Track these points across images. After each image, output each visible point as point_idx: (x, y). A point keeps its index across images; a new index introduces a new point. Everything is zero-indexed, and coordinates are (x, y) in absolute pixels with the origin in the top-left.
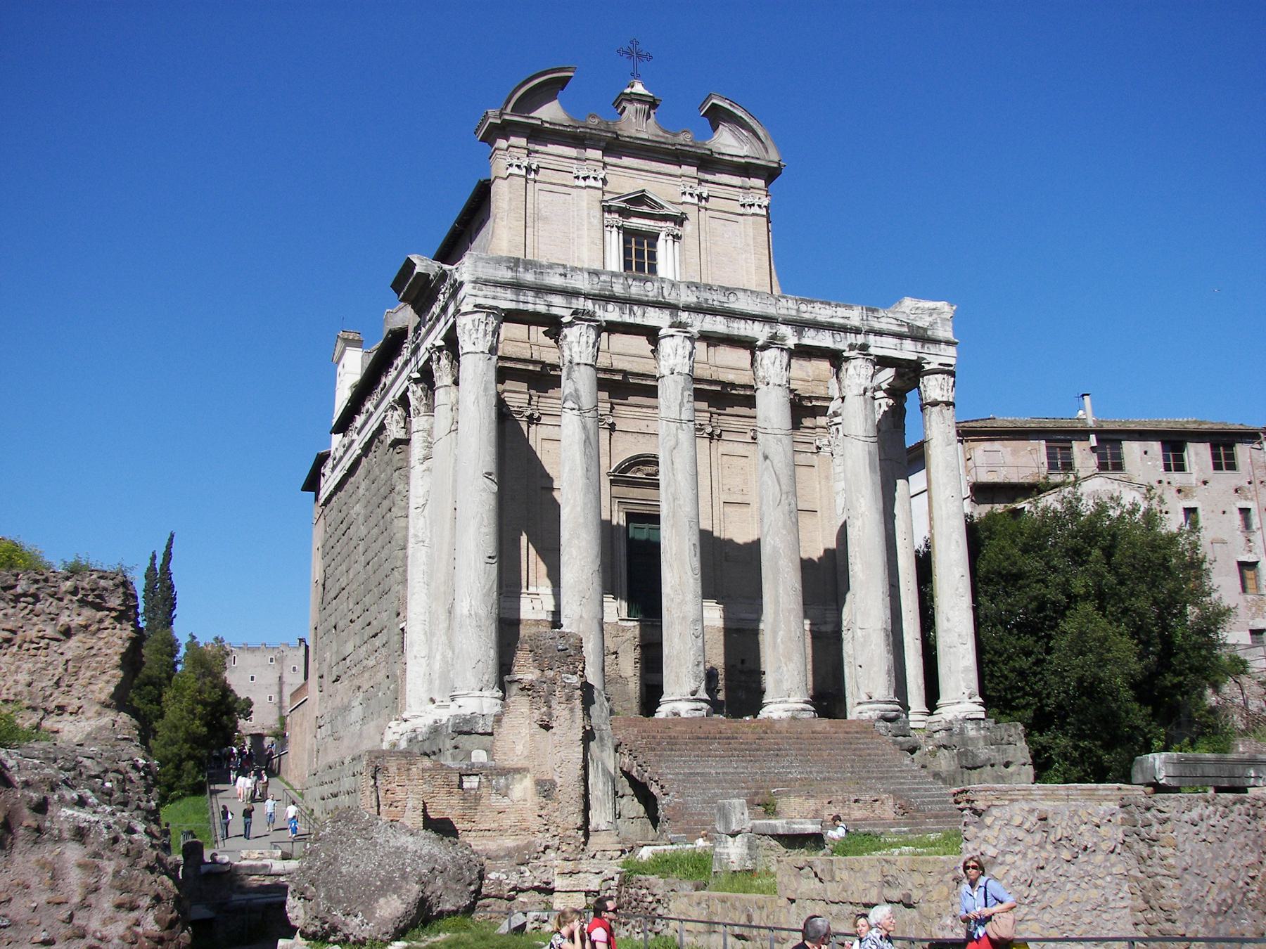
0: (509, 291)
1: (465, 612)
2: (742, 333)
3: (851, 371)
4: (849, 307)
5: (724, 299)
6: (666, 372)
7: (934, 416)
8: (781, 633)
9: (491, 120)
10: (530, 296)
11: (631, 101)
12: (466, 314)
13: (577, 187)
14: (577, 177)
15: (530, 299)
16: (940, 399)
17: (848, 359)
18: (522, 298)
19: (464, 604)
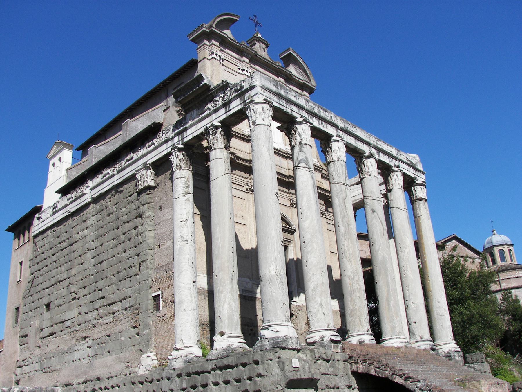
0: (276, 97)
1: (273, 273)
2: (361, 148)
3: (395, 177)
4: (392, 147)
5: (353, 129)
6: (335, 159)
7: (421, 205)
8: (392, 302)
9: (204, 29)
10: (284, 103)
11: (258, 41)
12: (258, 103)
13: (239, 73)
14: (239, 69)
15: (285, 105)
16: (423, 197)
17: (394, 171)
18: (281, 103)
19: (272, 268)
